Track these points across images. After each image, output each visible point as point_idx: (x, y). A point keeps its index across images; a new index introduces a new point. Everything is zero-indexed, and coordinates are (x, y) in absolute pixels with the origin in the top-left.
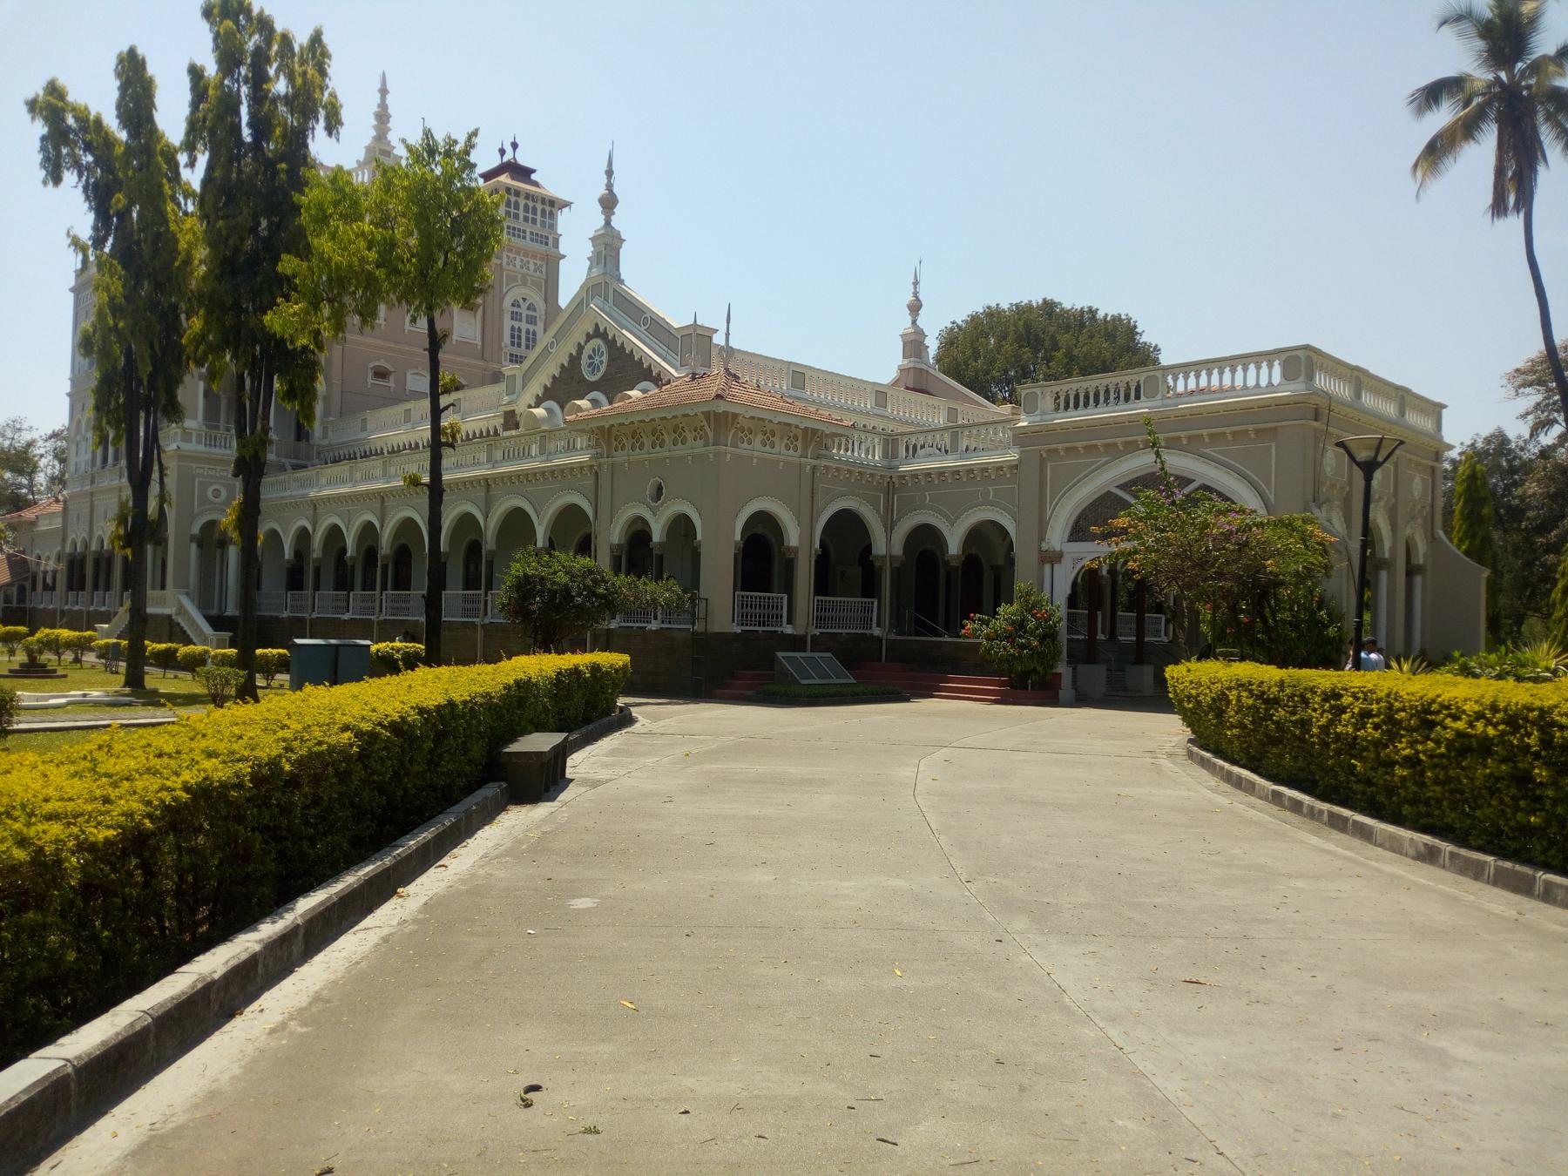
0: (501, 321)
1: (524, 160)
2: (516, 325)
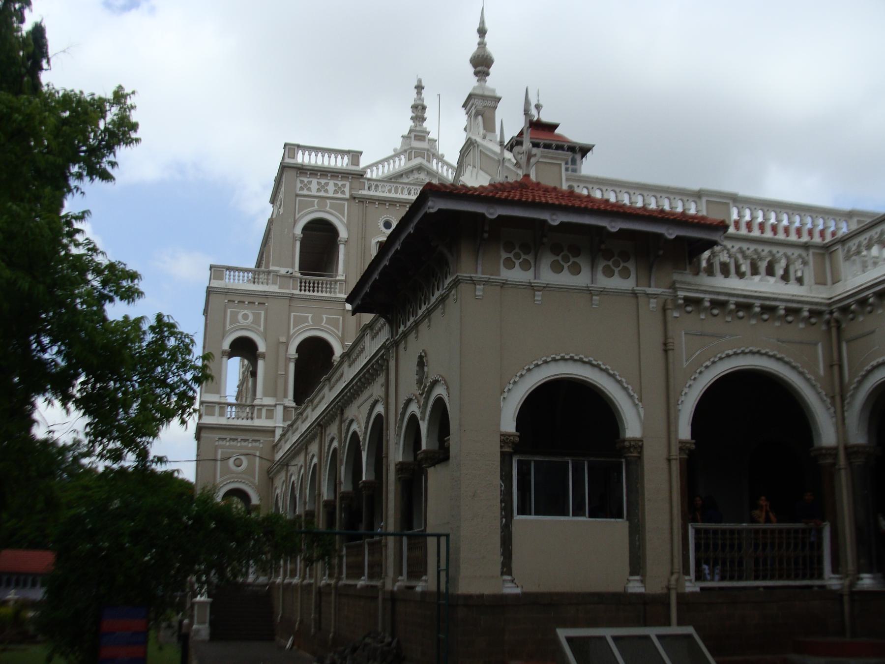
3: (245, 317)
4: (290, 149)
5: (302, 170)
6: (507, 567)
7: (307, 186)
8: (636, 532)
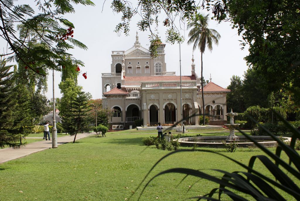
0: (154, 68)
2: (157, 68)
3: (108, 81)
4: (113, 52)
5: (115, 56)
6: (111, 121)
7: (116, 58)
8: (122, 118)
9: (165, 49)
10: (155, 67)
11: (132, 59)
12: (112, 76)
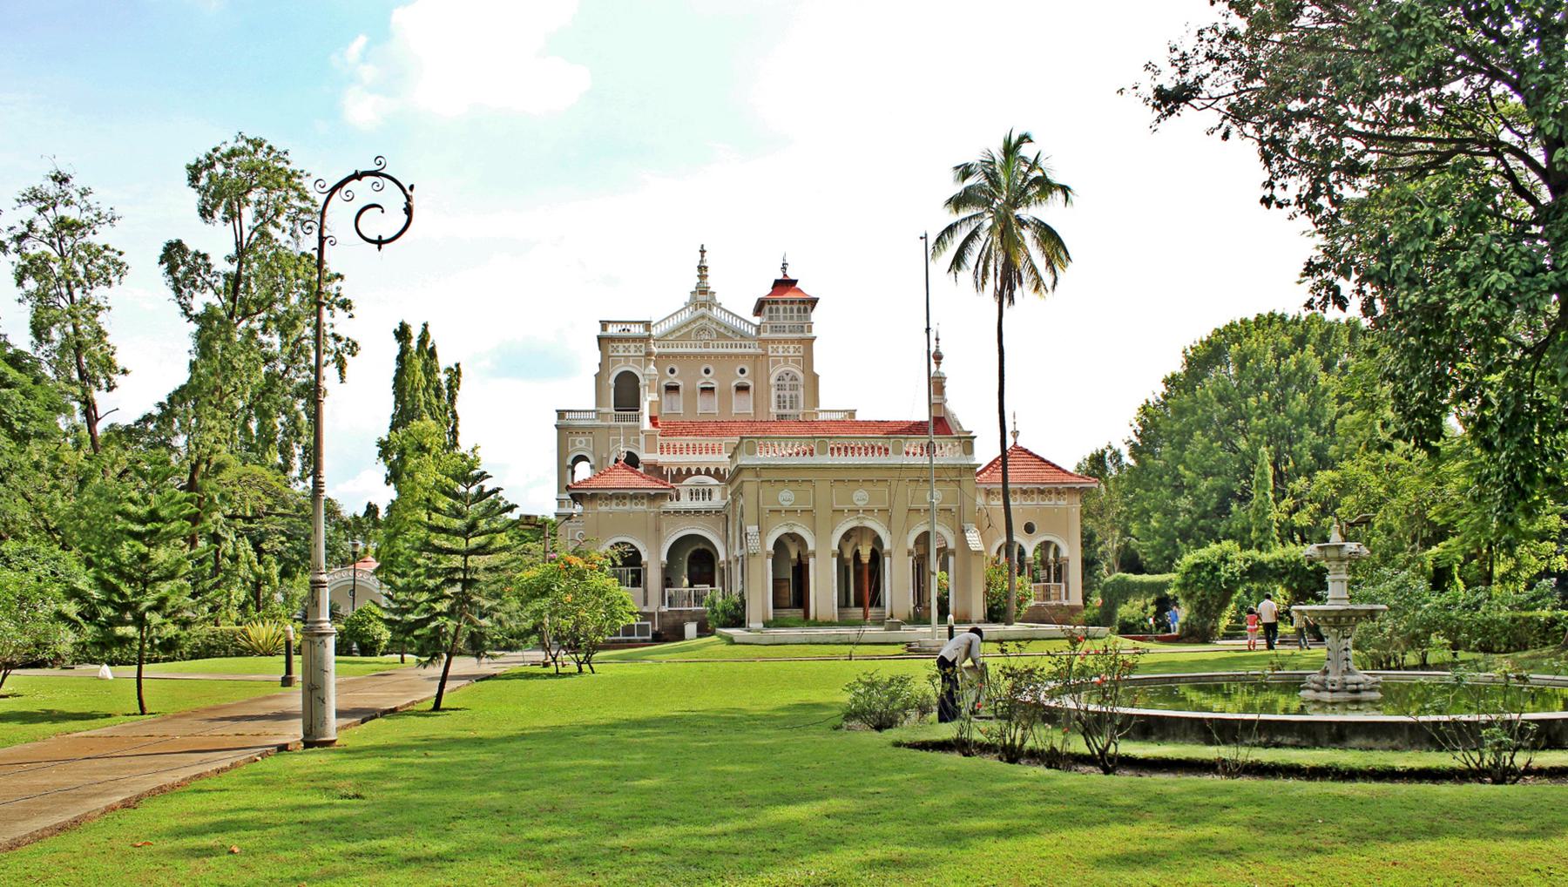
0: (769, 392)
1: (791, 276)
4: (604, 324)
5: (612, 339)
9: (816, 315)
10: (773, 390)
11: (682, 355)
12: (598, 422)
